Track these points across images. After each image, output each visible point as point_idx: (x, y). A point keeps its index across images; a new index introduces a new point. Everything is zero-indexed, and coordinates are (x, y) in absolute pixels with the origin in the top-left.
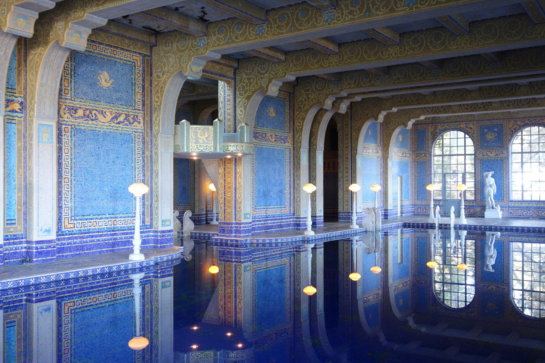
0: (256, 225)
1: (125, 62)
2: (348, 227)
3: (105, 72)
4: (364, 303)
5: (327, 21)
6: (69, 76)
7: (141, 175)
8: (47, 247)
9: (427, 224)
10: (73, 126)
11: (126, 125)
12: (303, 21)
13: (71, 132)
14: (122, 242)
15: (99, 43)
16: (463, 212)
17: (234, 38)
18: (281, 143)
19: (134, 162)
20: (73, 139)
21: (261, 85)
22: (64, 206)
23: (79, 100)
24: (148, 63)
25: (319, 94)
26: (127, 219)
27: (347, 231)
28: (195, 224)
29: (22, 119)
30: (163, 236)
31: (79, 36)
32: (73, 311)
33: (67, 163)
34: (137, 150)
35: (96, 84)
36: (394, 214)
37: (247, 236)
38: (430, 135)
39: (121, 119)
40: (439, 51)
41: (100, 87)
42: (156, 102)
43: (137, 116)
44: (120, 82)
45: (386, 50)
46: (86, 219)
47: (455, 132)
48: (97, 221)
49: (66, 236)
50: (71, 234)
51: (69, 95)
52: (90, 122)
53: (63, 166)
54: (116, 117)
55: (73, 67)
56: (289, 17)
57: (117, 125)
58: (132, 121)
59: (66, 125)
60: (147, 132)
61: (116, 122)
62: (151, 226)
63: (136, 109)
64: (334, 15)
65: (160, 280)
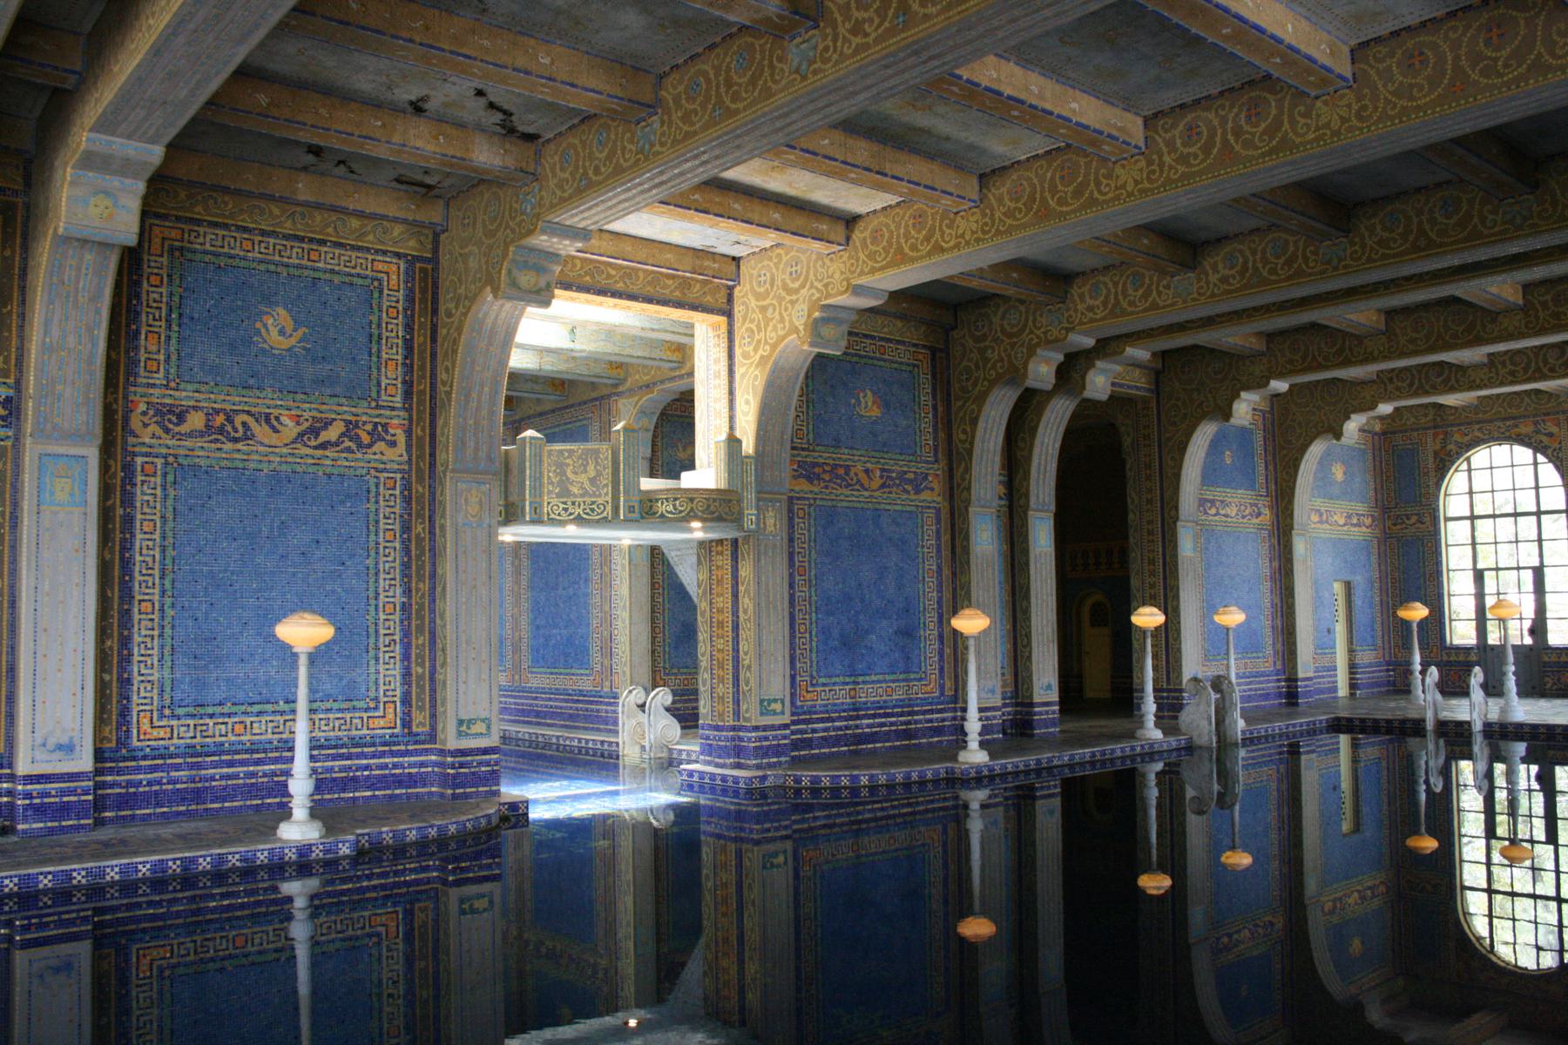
0: (814, 731)
1: (347, 279)
2: (1131, 735)
3: (282, 311)
5: (797, 71)
6: (163, 323)
7: (399, 591)
8: (63, 792)
9: (1404, 721)
10: (171, 459)
11: (349, 450)
12: (740, 85)
13: (165, 475)
14: (334, 779)
15: (263, 233)
16: (1511, 683)
17: (590, 172)
19: (372, 553)
20: (172, 493)
21: (791, 322)
22: (136, 679)
23: (190, 387)
24: (424, 279)
25: (1013, 345)
26: (348, 716)
27: (1118, 748)
28: (683, 728)
29: (9, 443)
30: (462, 765)
31: (108, 202)
32: (167, 973)
33: (149, 559)
34: (382, 521)
35: (248, 342)
36: (1321, 691)
37: (771, 766)
38: (1431, 460)
39: (332, 434)
40: (1263, 155)
41: (263, 350)
42: (444, 383)
43: (385, 426)
44: (331, 334)
45: (1109, 176)
46: (211, 716)
47: (1506, 447)
48: (248, 720)
49: (143, 763)
50: (162, 757)
51: (161, 375)
52: (228, 446)
53: (137, 569)
54: (315, 431)
55: (176, 299)
56: (708, 81)
57: (319, 453)
58: (366, 439)
59: (147, 455)
60: (419, 470)
61: (313, 443)
62: (432, 737)
63: (383, 407)
64: (815, 48)
65: (454, 893)
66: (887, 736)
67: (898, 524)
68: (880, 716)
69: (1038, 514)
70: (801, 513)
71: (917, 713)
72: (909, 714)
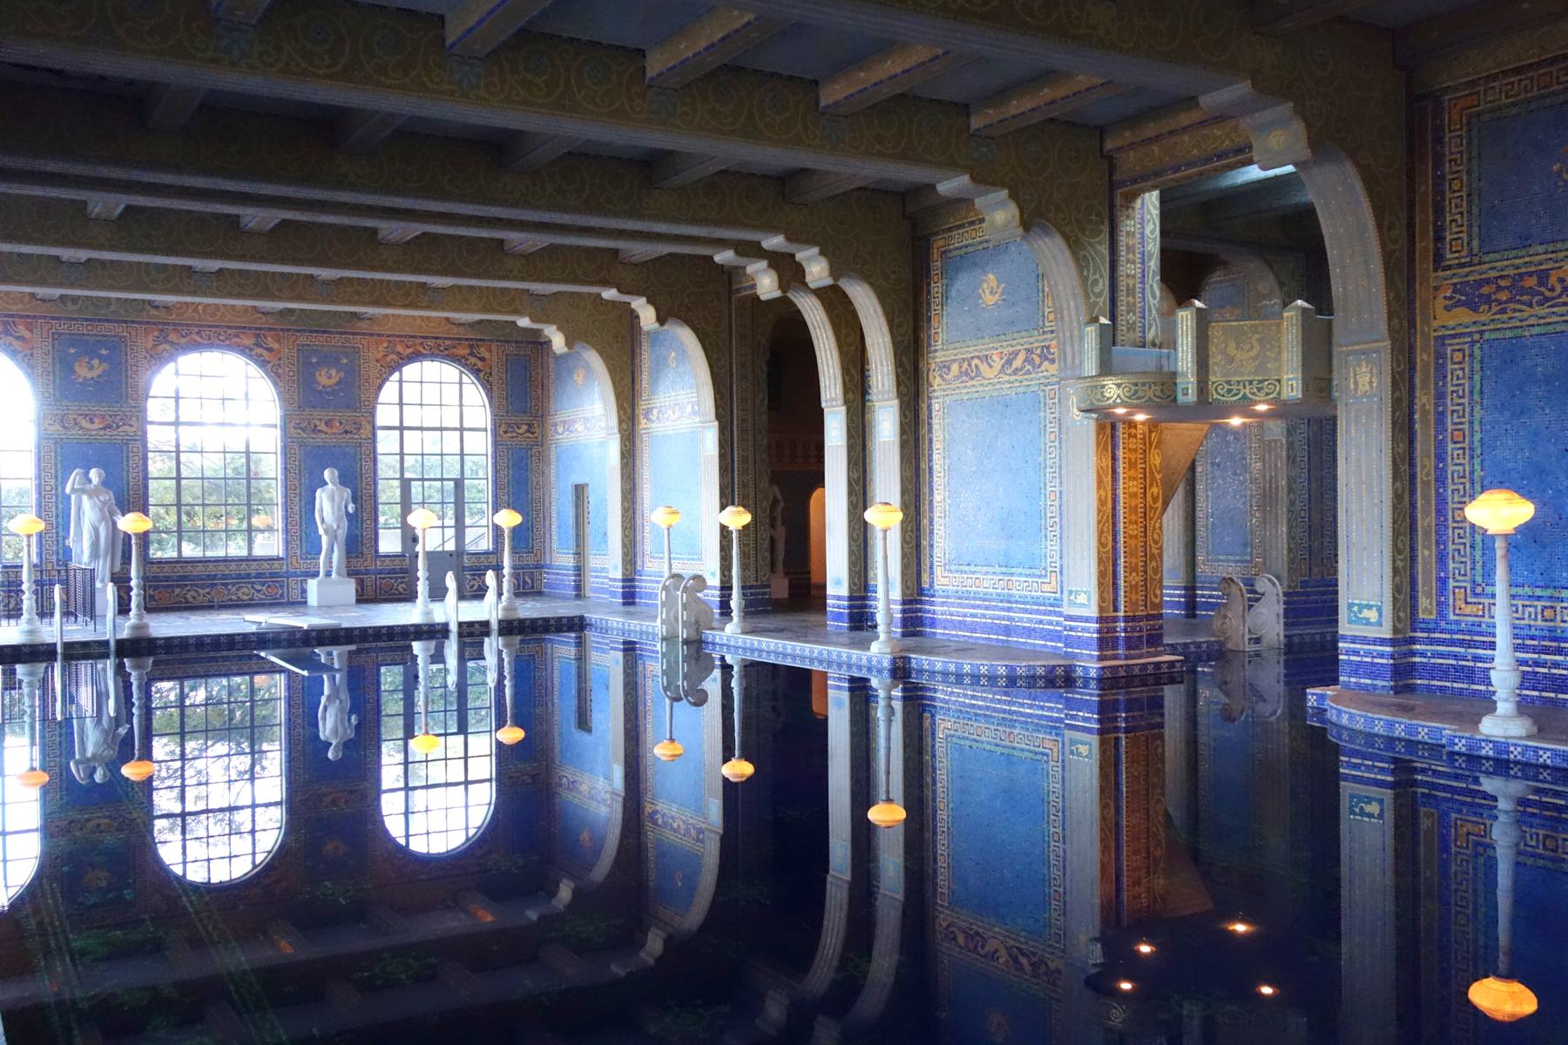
3: (991, 276)
11: (1028, 373)
39: (1017, 363)
43: (1048, 348)
54: (1009, 362)
58: (1037, 361)
70: (1458, 356)
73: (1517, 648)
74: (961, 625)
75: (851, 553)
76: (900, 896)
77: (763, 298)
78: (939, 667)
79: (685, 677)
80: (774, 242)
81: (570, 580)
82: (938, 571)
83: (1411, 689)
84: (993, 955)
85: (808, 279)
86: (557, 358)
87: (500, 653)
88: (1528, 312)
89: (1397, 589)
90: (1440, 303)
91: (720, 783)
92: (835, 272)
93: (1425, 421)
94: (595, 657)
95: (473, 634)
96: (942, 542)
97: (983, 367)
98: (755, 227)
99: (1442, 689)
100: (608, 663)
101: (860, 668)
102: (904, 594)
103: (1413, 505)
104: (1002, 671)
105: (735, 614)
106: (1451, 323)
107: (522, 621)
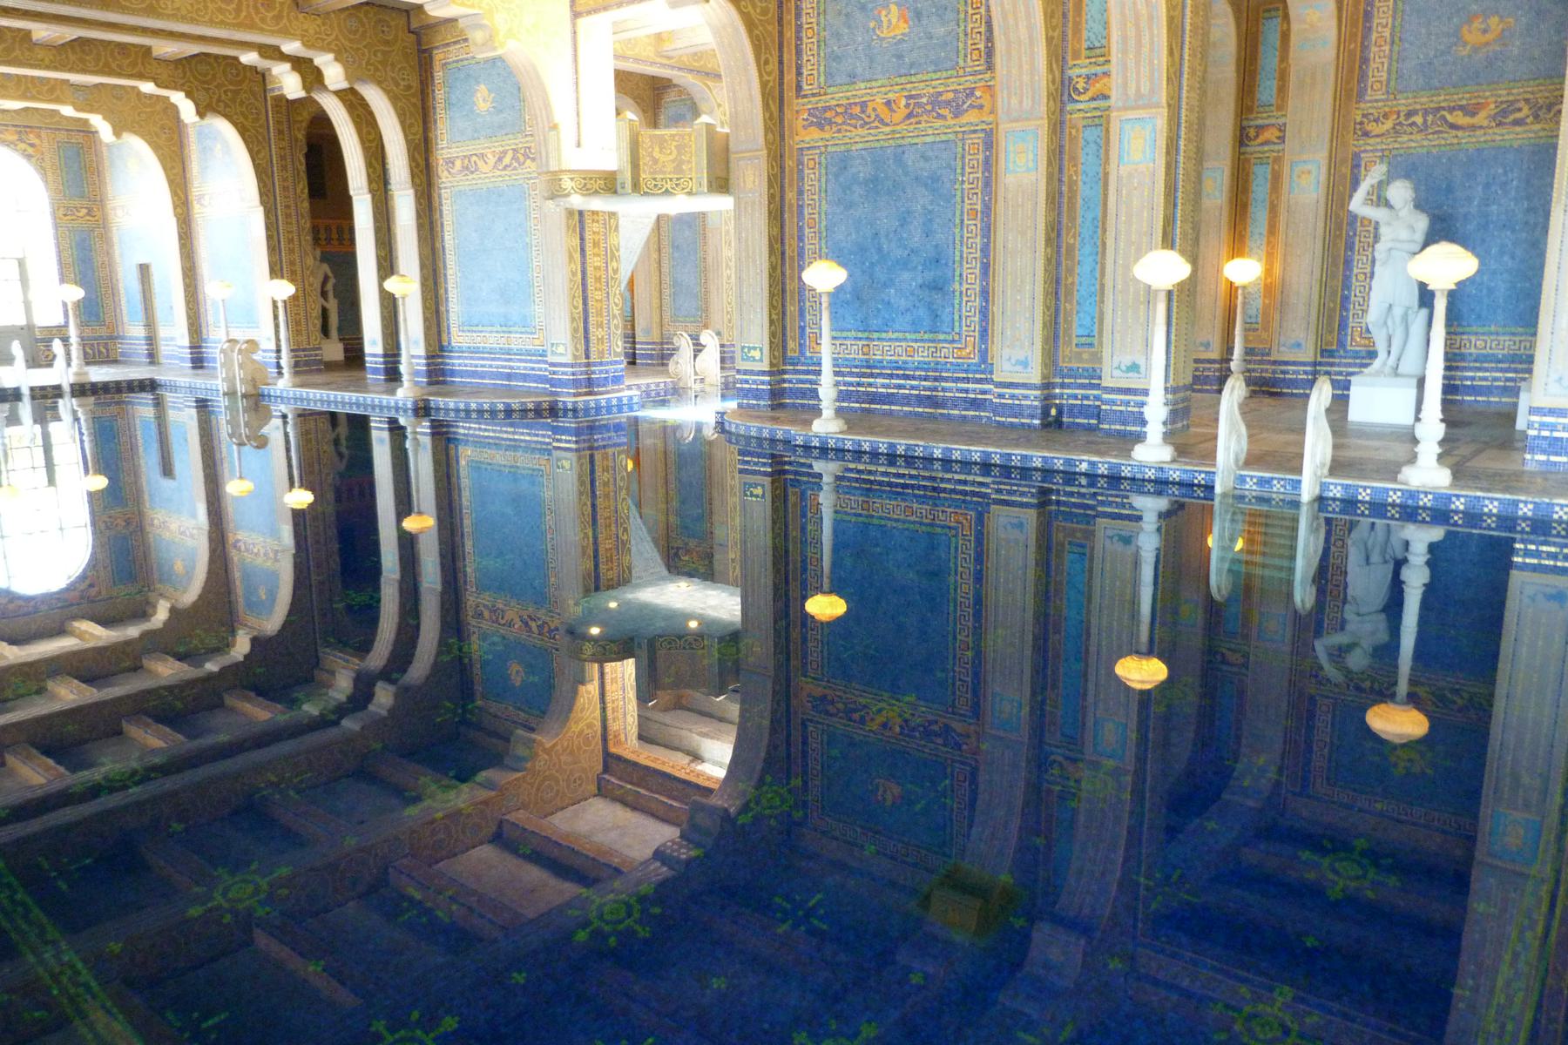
4: (571, 632)
18: (939, 116)
35: (472, 111)
39: (507, 160)
54: (500, 159)
58: (522, 159)
66: (906, 401)
67: (925, 158)
68: (898, 377)
69: (1131, 115)
71: (946, 379)
72: (936, 379)
73: (836, 374)
74: (474, 374)
75: (383, 318)
76: (439, 587)
77: (290, 97)
78: (452, 406)
79: (246, 425)
80: (291, 47)
81: (143, 349)
82: (454, 330)
83: (782, 406)
84: (510, 624)
85: (327, 82)
86: (107, 145)
87: (74, 412)
88: (855, 132)
89: (773, 335)
90: (800, 123)
91: (289, 514)
92: (348, 77)
93: (791, 212)
94: (172, 415)
95: (46, 398)
96: (455, 309)
97: (480, 163)
98: (272, 33)
99: (803, 405)
100: (183, 419)
101: (389, 408)
102: (427, 350)
103: (783, 274)
104: (501, 407)
105: (285, 371)
106: (807, 139)
107: (94, 385)
